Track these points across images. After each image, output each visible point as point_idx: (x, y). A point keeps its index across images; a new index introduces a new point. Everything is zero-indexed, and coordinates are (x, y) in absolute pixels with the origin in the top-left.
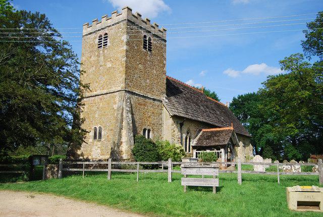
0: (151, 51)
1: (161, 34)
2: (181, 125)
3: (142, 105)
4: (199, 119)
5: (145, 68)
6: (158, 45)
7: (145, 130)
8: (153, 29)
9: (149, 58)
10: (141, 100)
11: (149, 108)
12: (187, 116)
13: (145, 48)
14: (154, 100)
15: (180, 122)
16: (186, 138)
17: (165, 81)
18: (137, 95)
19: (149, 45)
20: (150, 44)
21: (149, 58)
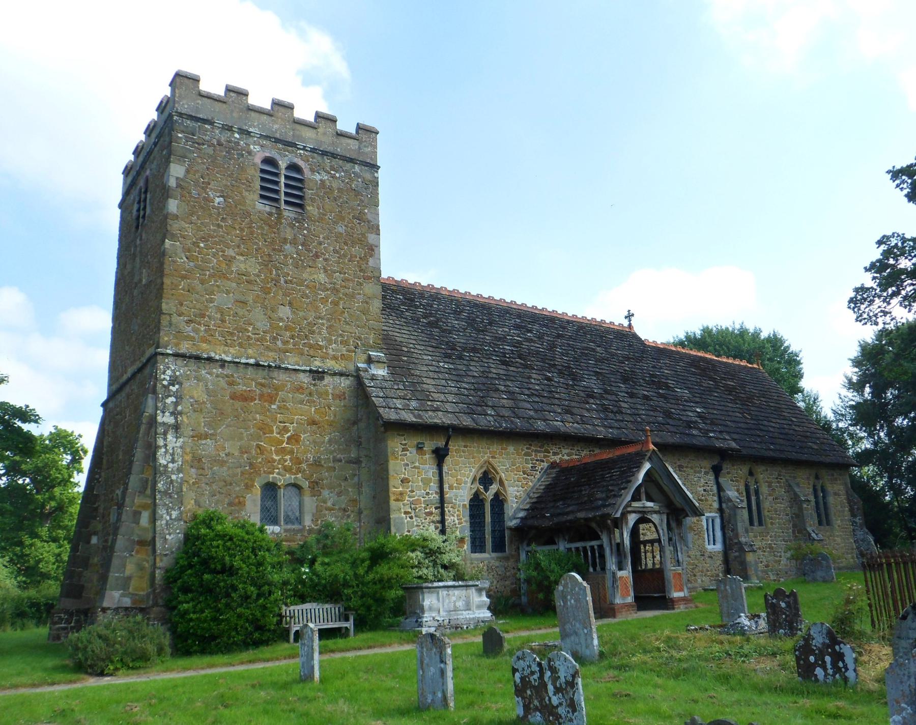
0: (301, 206)
1: (353, 144)
2: (440, 456)
3: (253, 399)
4: (540, 426)
5: (267, 263)
6: (335, 185)
7: (270, 489)
8: (308, 133)
9: (289, 234)
10: (248, 382)
11: (289, 405)
12: (467, 421)
13: (269, 193)
14: (318, 375)
15: (430, 444)
16: (476, 503)
17: (376, 305)
18: (223, 363)
19: (286, 185)
20: (296, 183)
21: (289, 234)
